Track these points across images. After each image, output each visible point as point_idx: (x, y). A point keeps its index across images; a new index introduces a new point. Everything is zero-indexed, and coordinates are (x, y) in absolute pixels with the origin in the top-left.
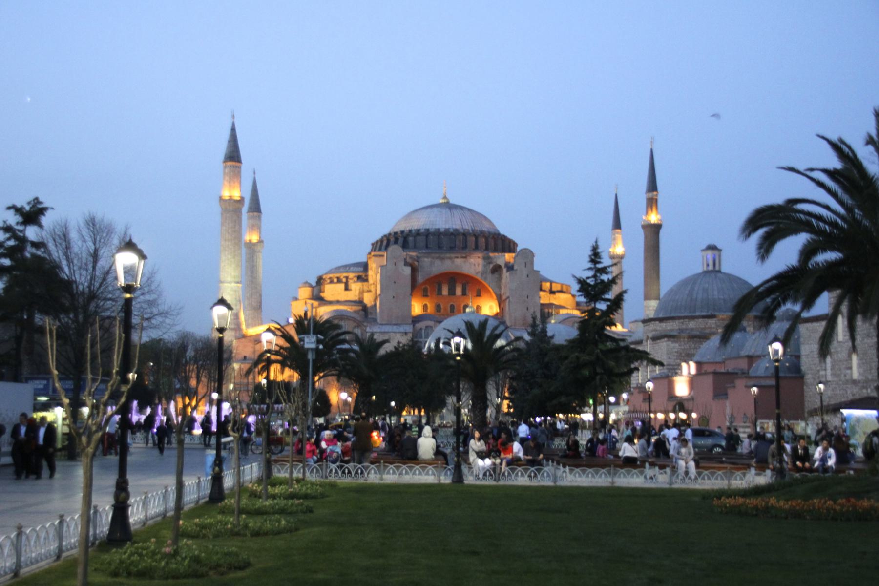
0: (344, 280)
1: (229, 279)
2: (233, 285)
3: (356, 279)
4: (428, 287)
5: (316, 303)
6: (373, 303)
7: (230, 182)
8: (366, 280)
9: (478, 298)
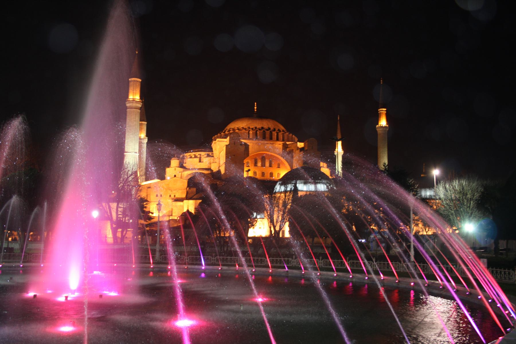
0: (199, 156)
1: (131, 151)
2: (133, 153)
3: (206, 155)
4: (250, 161)
5: (181, 169)
6: (217, 170)
7: (133, 91)
8: (213, 156)
9: (278, 168)
